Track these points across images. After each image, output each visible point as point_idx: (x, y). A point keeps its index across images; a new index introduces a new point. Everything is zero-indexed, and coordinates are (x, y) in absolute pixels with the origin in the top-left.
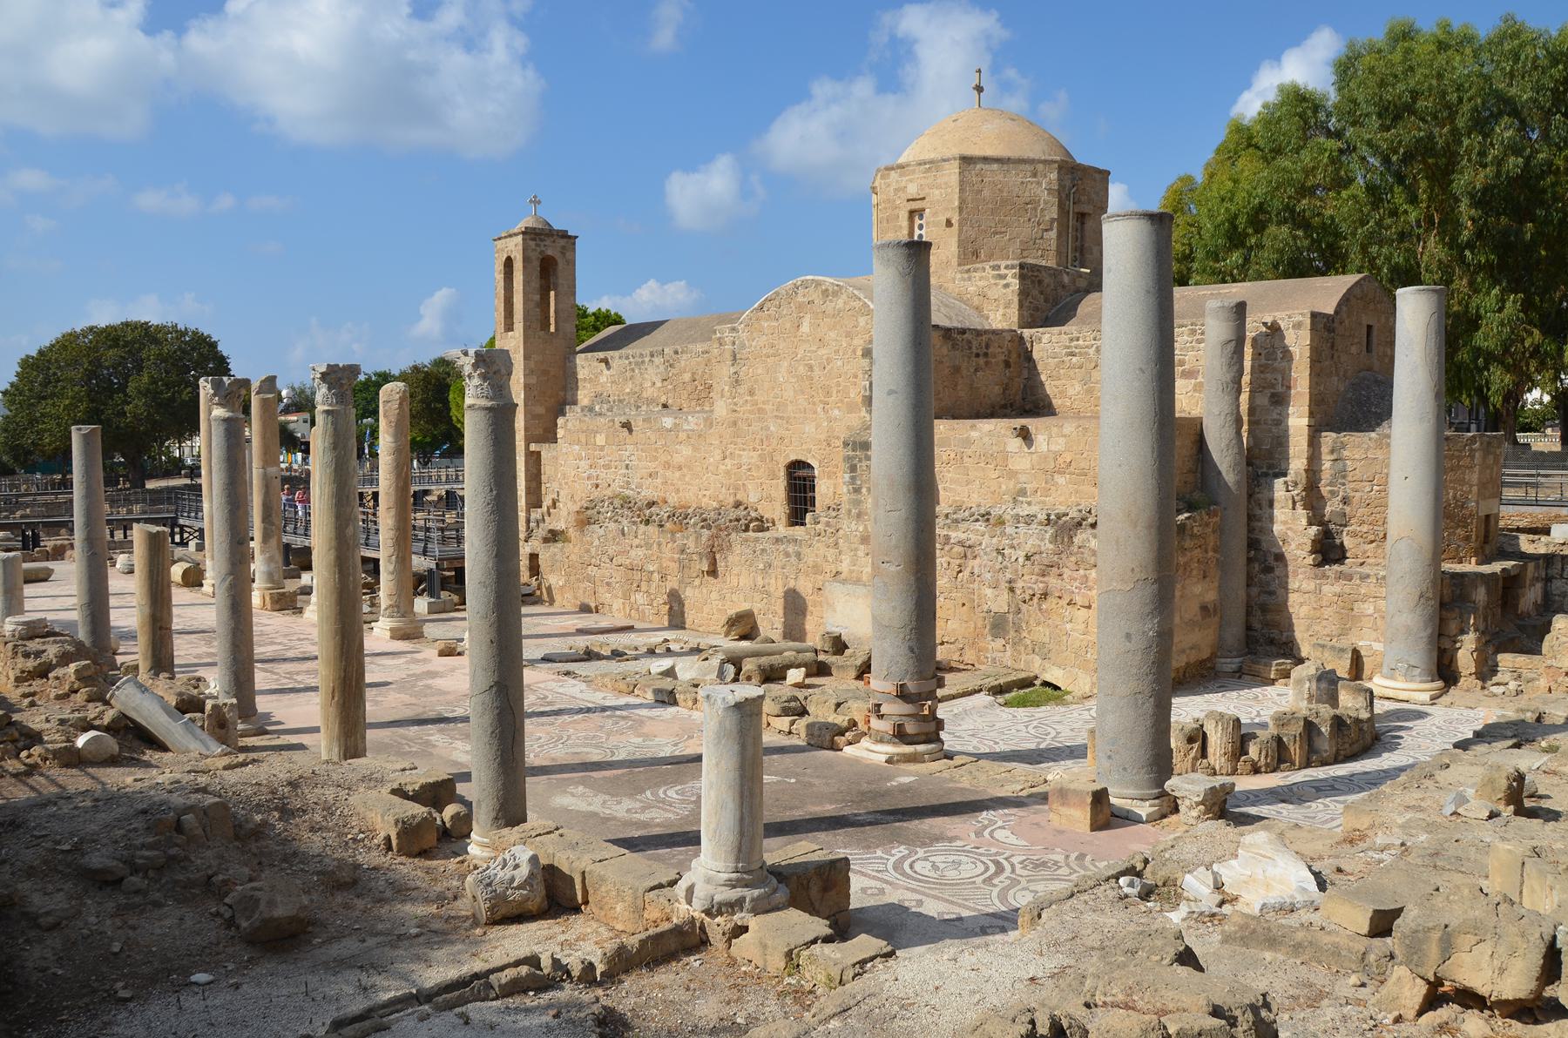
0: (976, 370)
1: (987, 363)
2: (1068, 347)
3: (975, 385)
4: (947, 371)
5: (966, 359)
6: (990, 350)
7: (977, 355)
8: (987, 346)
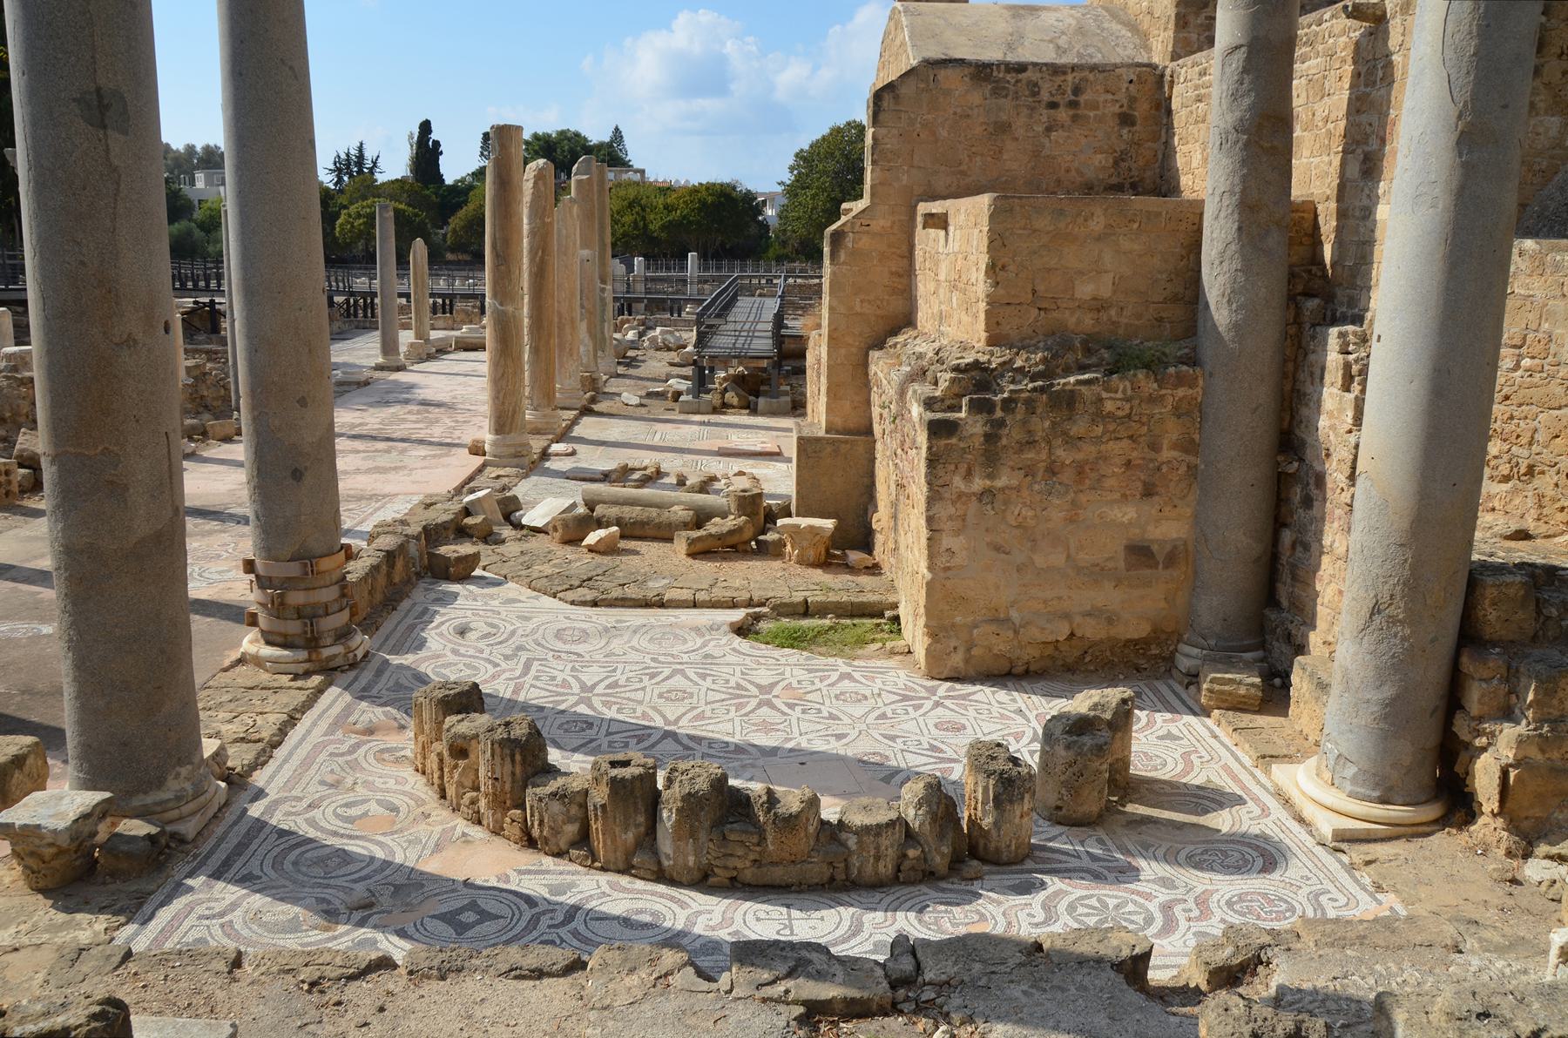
0: (1049, 129)
1: (1075, 118)
2: (1197, 87)
3: (1046, 152)
4: (978, 130)
5: (1025, 111)
6: (1082, 99)
7: (1053, 105)
8: (1077, 90)
